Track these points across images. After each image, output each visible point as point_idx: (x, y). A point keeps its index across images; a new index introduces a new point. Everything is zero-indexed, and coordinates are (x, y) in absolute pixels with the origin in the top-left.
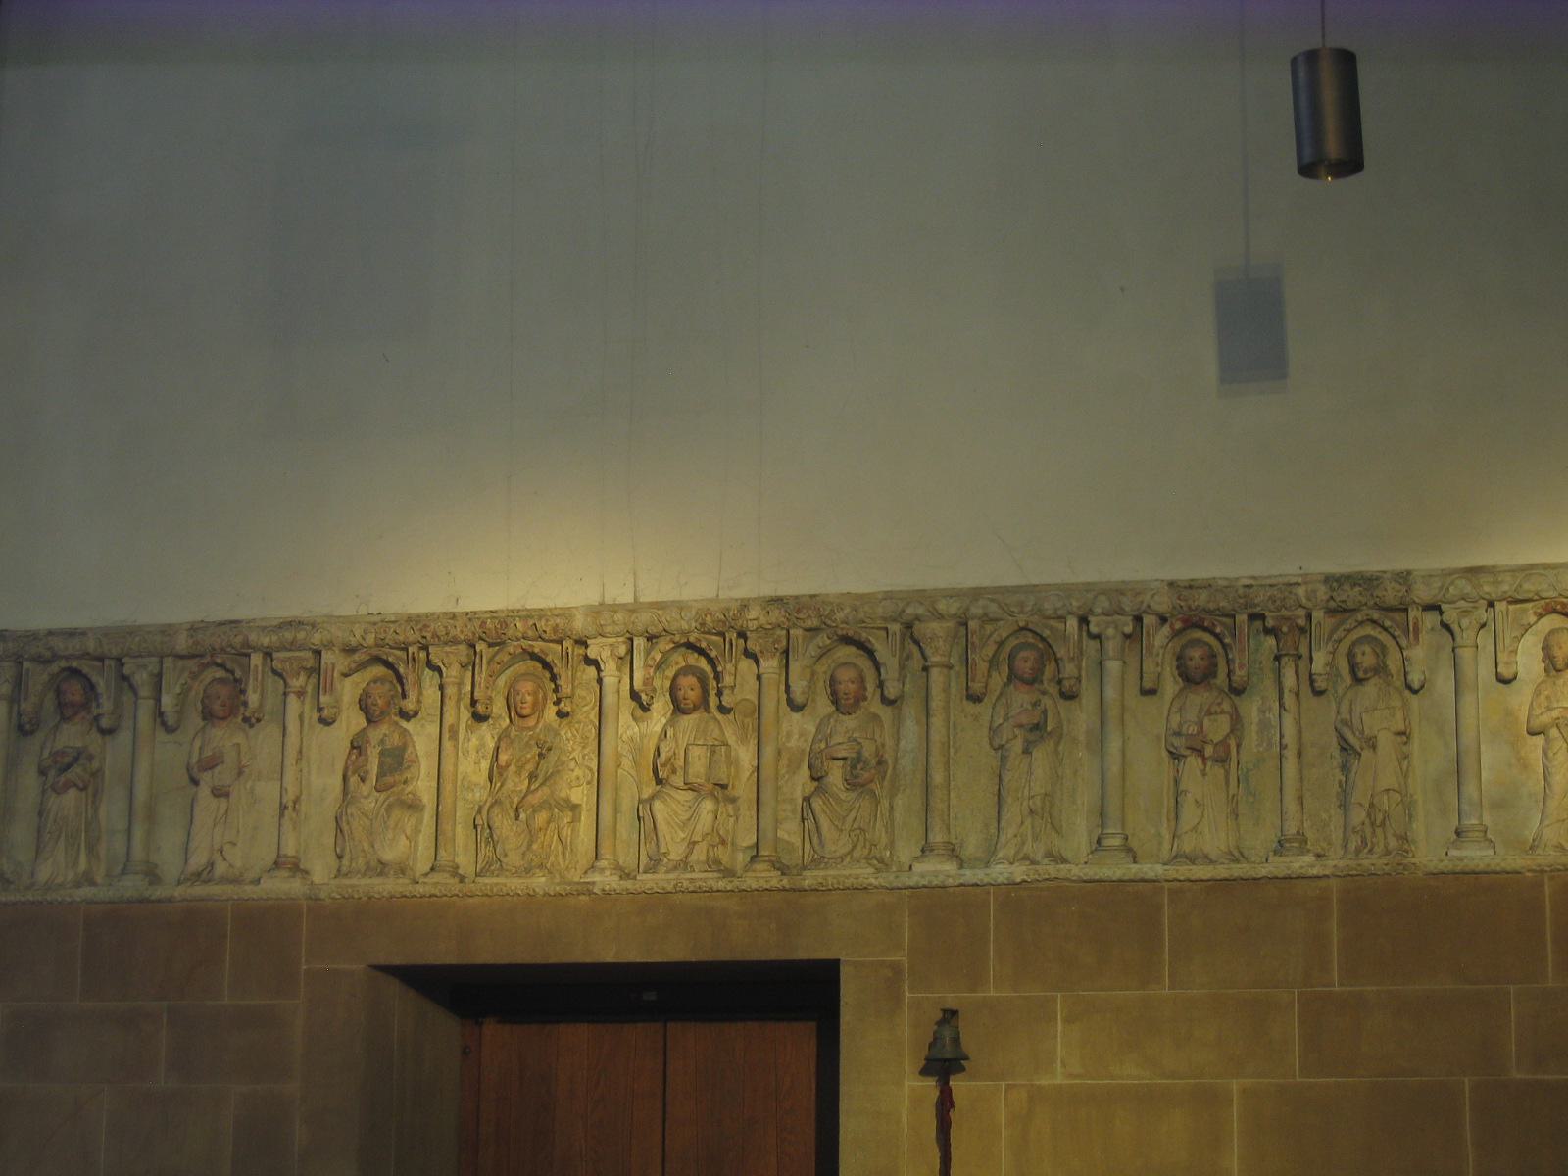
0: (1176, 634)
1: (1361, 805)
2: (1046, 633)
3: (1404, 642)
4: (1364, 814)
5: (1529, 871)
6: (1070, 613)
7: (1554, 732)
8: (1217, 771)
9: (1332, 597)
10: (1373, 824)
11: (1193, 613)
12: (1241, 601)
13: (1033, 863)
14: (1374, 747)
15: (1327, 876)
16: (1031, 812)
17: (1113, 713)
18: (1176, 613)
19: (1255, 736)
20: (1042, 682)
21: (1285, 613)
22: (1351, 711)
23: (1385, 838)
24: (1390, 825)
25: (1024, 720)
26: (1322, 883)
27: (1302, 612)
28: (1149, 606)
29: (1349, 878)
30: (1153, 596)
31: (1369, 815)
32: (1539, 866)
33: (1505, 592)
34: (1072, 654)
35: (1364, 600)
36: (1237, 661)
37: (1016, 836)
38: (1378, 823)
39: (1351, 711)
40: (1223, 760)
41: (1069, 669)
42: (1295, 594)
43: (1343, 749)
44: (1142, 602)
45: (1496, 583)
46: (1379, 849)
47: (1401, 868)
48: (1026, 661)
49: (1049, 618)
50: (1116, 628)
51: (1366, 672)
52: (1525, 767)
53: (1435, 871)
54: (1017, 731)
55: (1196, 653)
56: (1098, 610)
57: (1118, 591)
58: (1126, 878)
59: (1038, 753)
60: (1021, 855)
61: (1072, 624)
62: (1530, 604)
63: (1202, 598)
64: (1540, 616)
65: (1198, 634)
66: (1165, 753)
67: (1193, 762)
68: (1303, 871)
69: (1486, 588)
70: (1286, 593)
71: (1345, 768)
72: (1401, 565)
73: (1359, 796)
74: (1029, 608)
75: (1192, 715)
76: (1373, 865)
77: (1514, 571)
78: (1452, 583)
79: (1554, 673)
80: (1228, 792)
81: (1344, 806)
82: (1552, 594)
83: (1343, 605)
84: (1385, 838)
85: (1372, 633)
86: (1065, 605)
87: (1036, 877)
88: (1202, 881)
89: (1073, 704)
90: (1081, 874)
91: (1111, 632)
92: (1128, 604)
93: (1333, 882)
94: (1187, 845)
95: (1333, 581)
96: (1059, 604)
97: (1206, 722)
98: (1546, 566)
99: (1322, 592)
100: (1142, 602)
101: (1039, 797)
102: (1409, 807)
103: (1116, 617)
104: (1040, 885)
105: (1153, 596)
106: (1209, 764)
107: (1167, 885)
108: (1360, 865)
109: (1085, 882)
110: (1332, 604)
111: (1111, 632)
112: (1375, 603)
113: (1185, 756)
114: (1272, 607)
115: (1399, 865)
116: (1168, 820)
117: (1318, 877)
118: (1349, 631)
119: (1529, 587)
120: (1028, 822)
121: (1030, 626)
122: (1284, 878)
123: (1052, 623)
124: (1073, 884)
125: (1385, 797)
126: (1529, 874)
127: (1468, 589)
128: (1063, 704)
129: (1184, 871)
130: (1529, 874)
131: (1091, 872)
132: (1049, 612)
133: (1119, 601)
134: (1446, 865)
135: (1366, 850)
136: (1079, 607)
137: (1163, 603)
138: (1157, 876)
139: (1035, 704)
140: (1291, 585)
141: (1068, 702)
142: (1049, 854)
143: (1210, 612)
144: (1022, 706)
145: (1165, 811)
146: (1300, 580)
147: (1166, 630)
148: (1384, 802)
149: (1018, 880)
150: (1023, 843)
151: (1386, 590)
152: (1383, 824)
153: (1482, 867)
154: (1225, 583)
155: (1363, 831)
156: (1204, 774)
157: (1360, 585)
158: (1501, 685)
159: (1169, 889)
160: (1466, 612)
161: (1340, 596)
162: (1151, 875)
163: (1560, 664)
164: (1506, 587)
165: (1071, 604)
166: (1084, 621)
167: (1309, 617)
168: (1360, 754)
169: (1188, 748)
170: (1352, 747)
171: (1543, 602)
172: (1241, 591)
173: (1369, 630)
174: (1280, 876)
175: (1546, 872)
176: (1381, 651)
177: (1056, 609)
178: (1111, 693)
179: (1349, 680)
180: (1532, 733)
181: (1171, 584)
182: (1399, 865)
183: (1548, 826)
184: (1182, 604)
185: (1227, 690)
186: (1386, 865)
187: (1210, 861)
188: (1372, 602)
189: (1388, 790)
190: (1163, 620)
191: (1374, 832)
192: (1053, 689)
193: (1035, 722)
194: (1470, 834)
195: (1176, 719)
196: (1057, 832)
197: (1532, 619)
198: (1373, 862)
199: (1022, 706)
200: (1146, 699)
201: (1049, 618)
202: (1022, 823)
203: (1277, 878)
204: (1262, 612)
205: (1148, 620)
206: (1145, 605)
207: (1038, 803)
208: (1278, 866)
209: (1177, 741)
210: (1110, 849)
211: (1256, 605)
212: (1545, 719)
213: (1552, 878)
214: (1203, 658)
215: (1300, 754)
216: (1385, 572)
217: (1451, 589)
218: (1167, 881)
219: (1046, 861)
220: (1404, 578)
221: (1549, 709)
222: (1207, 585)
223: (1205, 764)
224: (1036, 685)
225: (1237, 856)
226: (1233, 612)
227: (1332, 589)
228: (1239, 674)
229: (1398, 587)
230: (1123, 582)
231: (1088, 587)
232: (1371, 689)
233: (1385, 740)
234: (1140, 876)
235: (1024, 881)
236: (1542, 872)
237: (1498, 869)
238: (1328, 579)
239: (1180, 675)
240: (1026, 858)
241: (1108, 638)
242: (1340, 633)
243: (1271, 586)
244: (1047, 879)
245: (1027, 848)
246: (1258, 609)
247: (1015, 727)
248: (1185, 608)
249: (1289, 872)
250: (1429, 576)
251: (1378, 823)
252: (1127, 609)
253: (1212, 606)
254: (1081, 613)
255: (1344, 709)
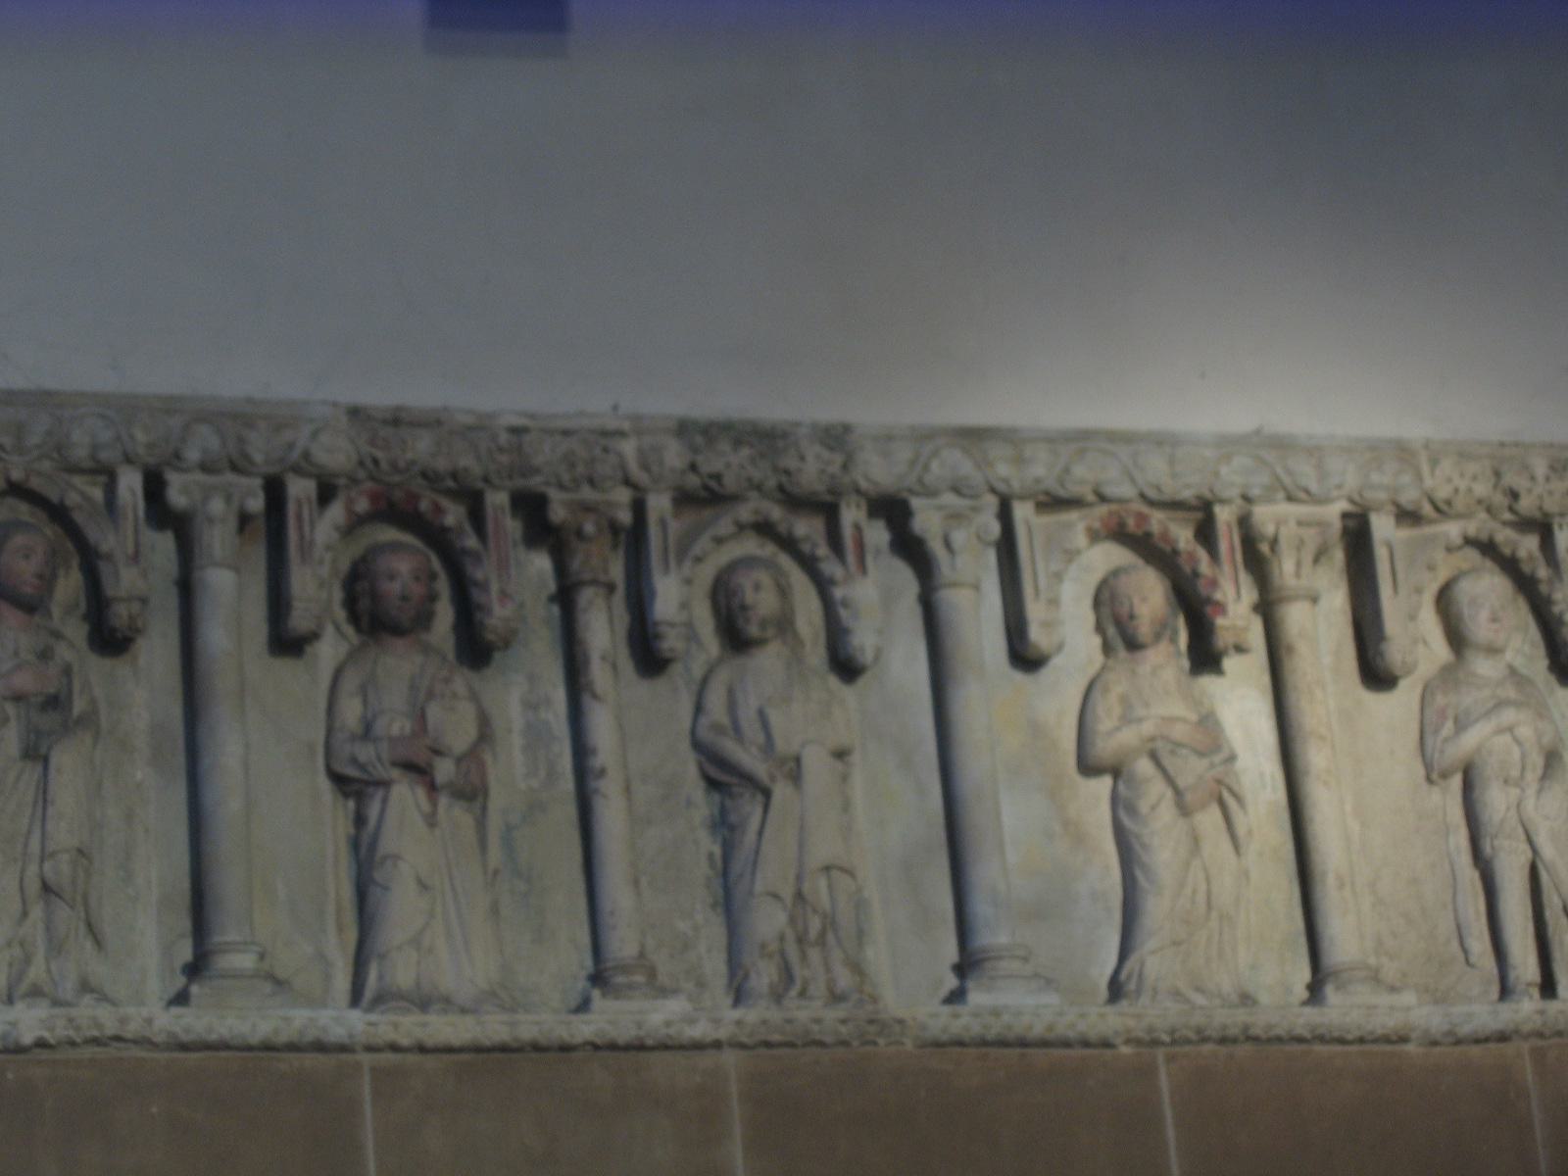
0: (354, 525)
1: (776, 896)
2: (72, 499)
3: (830, 568)
4: (780, 918)
5: (1128, 1042)
6: (129, 460)
7: (1144, 767)
8: (456, 816)
9: (693, 467)
10: (801, 940)
11: (397, 478)
12: (504, 459)
13: (56, 1003)
14: (796, 776)
15: (717, 1045)
16: (46, 888)
17: (221, 680)
18: (361, 474)
19: (518, 757)
20: (49, 614)
21: (587, 494)
22: (732, 706)
23: (828, 969)
24: (839, 942)
25: (24, 681)
26: (706, 1060)
27: (623, 495)
28: (306, 455)
29: (763, 1051)
30: (315, 434)
31: (792, 920)
32: (1151, 1030)
33: (1038, 481)
34: (131, 550)
35: (756, 475)
36: (494, 587)
37: (9, 944)
38: (813, 933)
39: (732, 706)
40: (472, 793)
41: (124, 582)
42: (620, 455)
43: (712, 784)
44: (291, 446)
45: (1020, 461)
46: (819, 989)
47: (872, 1029)
48: (27, 557)
49: (74, 469)
50: (228, 499)
51: (763, 624)
52: (1079, 837)
53: (945, 1038)
54: (10, 709)
55: (403, 566)
56: (193, 455)
57: (237, 418)
58: (283, 1039)
59: (66, 759)
60: (24, 987)
61: (130, 484)
62: (1072, 516)
63: (421, 447)
64: (1094, 537)
65: (389, 534)
66: (324, 784)
67: (406, 796)
68: (672, 1031)
69: (1003, 469)
70: (597, 451)
71: (725, 827)
72: (829, 413)
73: (773, 873)
74: (33, 439)
75: (394, 698)
76: (818, 1021)
77: (1055, 439)
78: (935, 453)
79: (1122, 653)
80: (485, 865)
81: (729, 903)
82: (1126, 491)
83: (713, 484)
84: (828, 969)
85: (759, 552)
86: (118, 438)
87: (71, 1033)
88: (449, 1050)
89: (120, 667)
90: (177, 1029)
91: (217, 506)
92: (260, 449)
93: (729, 1058)
94: (403, 973)
95: (695, 433)
96: (106, 436)
97: (434, 712)
98: (1114, 437)
99: (674, 456)
100: (291, 446)
101: (65, 857)
102: (860, 905)
103: (230, 477)
104: (72, 1054)
105: (315, 434)
106: (443, 801)
107: (366, 1059)
108: (789, 1021)
109: (184, 1047)
110: (693, 481)
111: (217, 506)
112: (781, 488)
113: (386, 784)
114: (566, 477)
115: (871, 1022)
116: (340, 929)
117: (698, 1046)
118: (719, 541)
119: (1083, 476)
120: (37, 912)
121: (36, 483)
122: (628, 1048)
123: (78, 480)
124: (156, 1055)
125: (823, 883)
126: (1125, 1050)
127: (966, 468)
128: (96, 669)
129: (408, 1026)
130: (1125, 1050)
131: (197, 1021)
132: (80, 453)
133: (241, 440)
134: (963, 1022)
135: (793, 993)
136: (150, 446)
137: (336, 452)
138: (351, 1036)
139: (45, 655)
140: (605, 434)
141: (107, 663)
142: (85, 987)
143: (430, 477)
144: (16, 654)
145: (331, 908)
146: (626, 426)
147: (336, 512)
148: (819, 889)
149: (27, 1039)
150: (27, 960)
151: (802, 458)
152: (821, 940)
153: (1038, 1030)
154: (469, 420)
155: (782, 954)
156: (431, 821)
157: (752, 446)
158: (1019, 677)
159: (373, 1070)
160: (956, 517)
161: (711, 464)
162: (337, 1033)
163: (1144, 629)
164: (1038, 470)
165: (132, 437)
166: (154, 487)
167: (639, 508)
168: (767, 793)
169: (395, 764)
170: (748, 779)
171: (1102, 510)
172: (504, 438)
173: (751, 546)
174: (621, 1041)
175: (1163, 1044)
176: (784, 591)
177: (95, 448)
178: (216, 636)
179: (712, 644)
180: (1088, 767)
181: (355, 413)
182: (871, 1022)
183: (1153, 952)
184: (380, 454)
185: (451, 656)
186: (844, 1022)
187: (447, 1003)
188: (771, 483)
189: (827, 869)
190: (326, 494)
191: (804, 957)
192: (77, 632)
193: (52, 690)
194: (1003, 964)
195: (351, 711)
196: (98, 943)
197: (1080, 539)
198: (808, 1013)
199: (16, 654)
200: (285, 666)
201: (74, 469)
202: (25, 914)
203: (613, 1047)
204: (543, 489)
205: (300, 489)
206: (295, 455)
207: (65, 868)
208: (611, 1018)
209: (365, 752)
210: (237, 975)
211: (537, 471)
212: (1128, 737)
213: (1171, 1059)
214: (417, 579)
215: (628, 789)
216: (797, 424)
217: (935, 465)
218: (370, 1049)
219: (87, 999)
220: (836, 437)
221: (1127, 719)
222: (432, 421)
223: (434, 804)
224: (37, 618)
225: (502, 996)
226: (480, 485)
227: (695, 450)
228: (497, 615)
229: (826, 454)
230: (249, 400)
231: (169, 405)
232: (769, 660)
233: (816, 763)
234: (311, 1035)
235: (41, 1044)
236: (1155, 1043)
237: (1071, 1034)
238: (684, 429)
239: (354, 617)
240: (36, 992)
241: (211, 520)
242: (703, 543)
243: (566, 433)
244: (95, 1041)
245: (36, 972)
246: (535, 482)
247: (5, 699)
248: (384, 465)
249: (642, 1033)
250: (886, 439)
251: (813, 933)
252: (258, 458)
253: (442, 464)
254: (151, 460)
255: (716, 701)
